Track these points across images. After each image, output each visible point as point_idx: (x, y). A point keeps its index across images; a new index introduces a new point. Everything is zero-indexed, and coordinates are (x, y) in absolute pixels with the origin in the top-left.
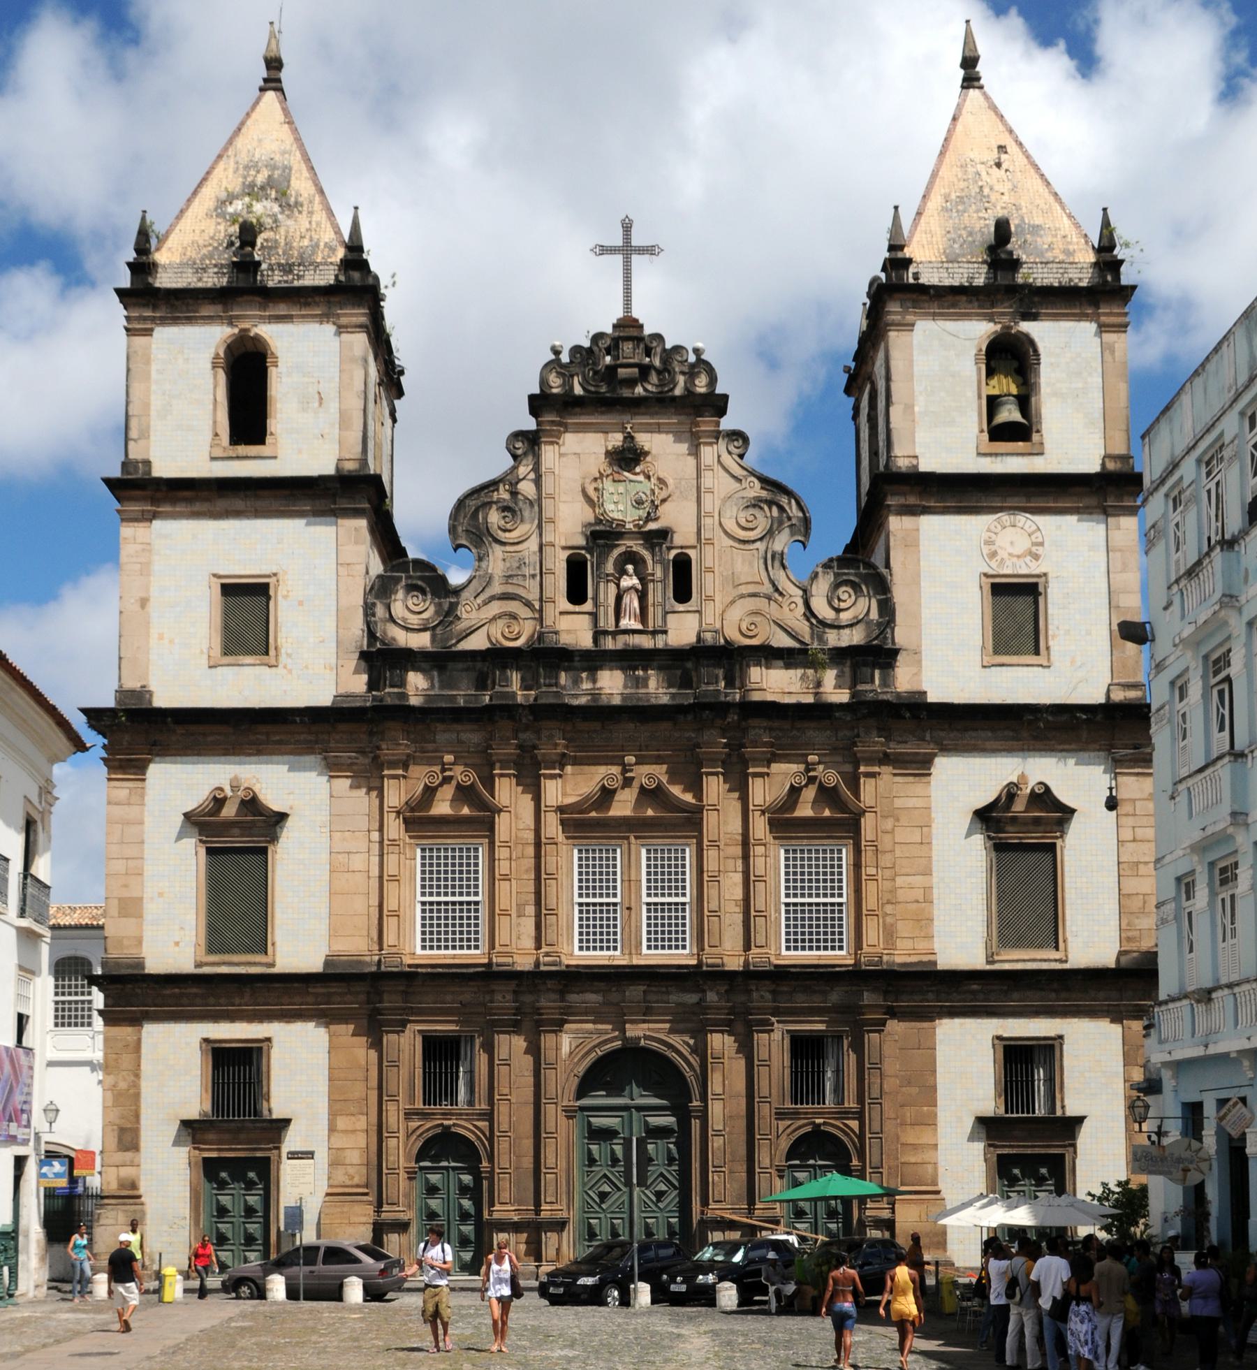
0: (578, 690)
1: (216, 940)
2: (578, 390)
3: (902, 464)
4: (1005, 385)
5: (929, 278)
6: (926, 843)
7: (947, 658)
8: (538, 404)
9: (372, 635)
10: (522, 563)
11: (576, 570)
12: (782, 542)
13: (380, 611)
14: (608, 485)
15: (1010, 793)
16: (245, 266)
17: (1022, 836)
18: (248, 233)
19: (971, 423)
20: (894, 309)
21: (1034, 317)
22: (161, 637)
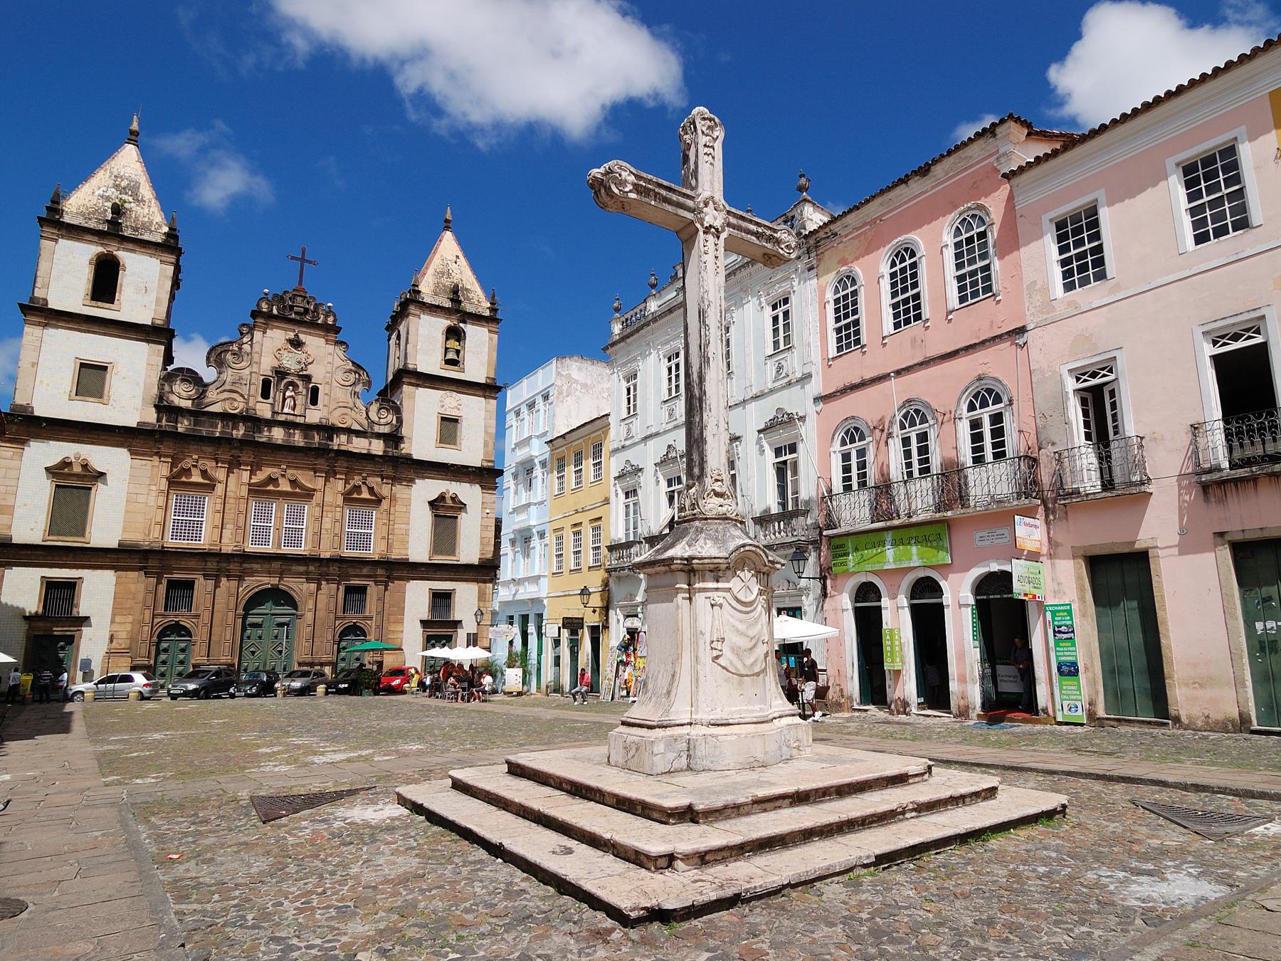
0: (263, 437)
1: (53, 528)
2: (275, 312)
3: (411, 366)
4: (453, 344)
5: (428, 300)
6: (408, 512)
7: (422, 443)
8: (255, 314)
9: (161, 398)
10: (240, 378)
11: (266, 384)
12: (359, 388)
13: (167, 388)
14: (286, 353)
15: (442, 498)
16: (114, 224)
17: (445, 513)
18: (117, 210)
19: (438, 356)
20: (412, 309)
21: (465, 322)
22: (42, 382)
